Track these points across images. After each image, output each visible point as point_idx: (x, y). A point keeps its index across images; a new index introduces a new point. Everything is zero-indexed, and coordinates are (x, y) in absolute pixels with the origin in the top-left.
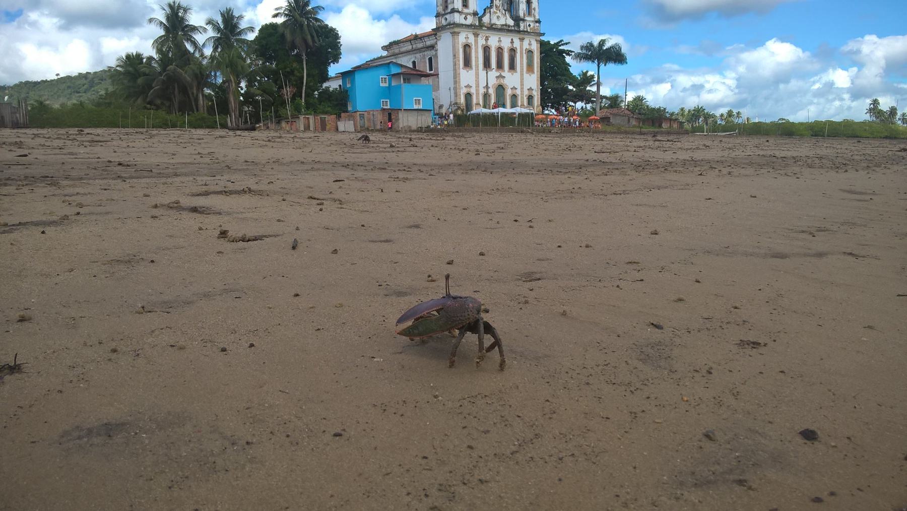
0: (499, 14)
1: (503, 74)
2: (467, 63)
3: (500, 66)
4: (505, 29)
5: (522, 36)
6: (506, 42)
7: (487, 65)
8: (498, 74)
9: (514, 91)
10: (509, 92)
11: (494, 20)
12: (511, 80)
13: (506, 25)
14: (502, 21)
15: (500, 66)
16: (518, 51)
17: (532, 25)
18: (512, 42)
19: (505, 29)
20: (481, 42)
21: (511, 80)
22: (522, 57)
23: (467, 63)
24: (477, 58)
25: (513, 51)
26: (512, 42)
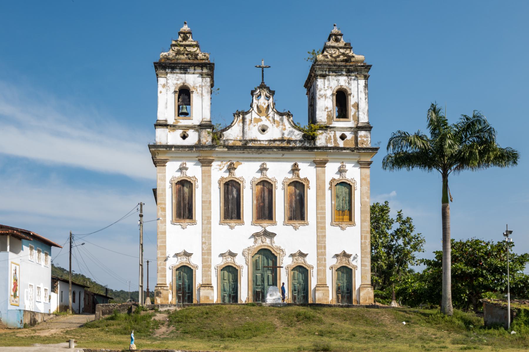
0: (265, 122)
1: (270, 229)
2: (185, 211)
3: (265, 212)
4: (282, 148)
5: (320, 158)
6: (279, 171)
7: (232, 211)
8: (258, 229)
9: (300, 261)
10: (286, 262)
11: (253, 133)
12: (290, 240)
13: (282, 140)
14: (274, 133)
15: (265, 212)
16: (313, 184)
17: (349, 136)
18: (295, 169)
19: (282, 148)
20: (218, 172)
21: (290, 240)
22: (320, 196)
23: (185, 211)
24: (207, 204)
25: (298, 187)
26: (295, 169)
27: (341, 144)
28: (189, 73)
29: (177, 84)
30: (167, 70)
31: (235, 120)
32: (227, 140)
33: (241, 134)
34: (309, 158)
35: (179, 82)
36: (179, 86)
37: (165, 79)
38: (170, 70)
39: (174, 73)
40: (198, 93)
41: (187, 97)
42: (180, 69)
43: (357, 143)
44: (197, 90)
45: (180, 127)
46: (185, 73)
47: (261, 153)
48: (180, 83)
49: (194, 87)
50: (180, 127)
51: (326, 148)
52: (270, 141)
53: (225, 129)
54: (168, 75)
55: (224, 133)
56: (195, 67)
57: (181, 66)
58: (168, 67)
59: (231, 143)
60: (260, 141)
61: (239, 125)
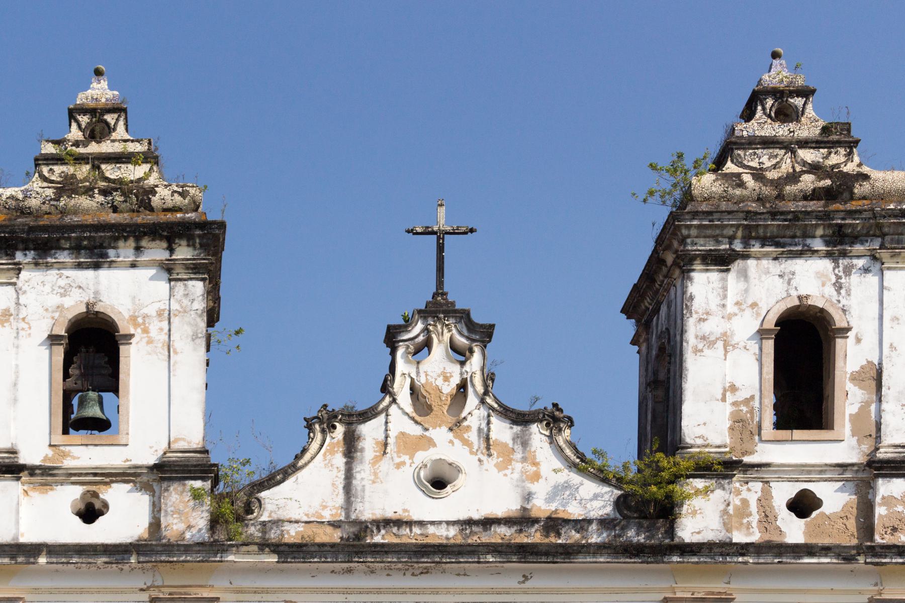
27: (794, 530)
28: (111, 264)
29: (60, 308)
30: (19, 256)
31: (315, 446)
32: (278, 522)
33: (340, 499)
34: (647, 591)
35: (68, 302)
36: (71, 315)
37: (10, 289)
38: (31, 254)
39: (49, 266)
40: (150, 342)
41: (102, 360)
42: (76, 249)
43: (867, 526)
44: (146, 331)
45: (72, 476)
46: (97, 266)
47: (426, 571)
48: (74, 305)
49: (133, 319)
50: (72, 476)
51: (720, 550)
52: (470, 522)
53: (271, 481)
54: (24, 274)
55: (263, 494)
56: (138, 239)
57: (80, 239)
58: (24, 241)
59: (292, 534)
60: (421, 523)
61: (329, 465)
